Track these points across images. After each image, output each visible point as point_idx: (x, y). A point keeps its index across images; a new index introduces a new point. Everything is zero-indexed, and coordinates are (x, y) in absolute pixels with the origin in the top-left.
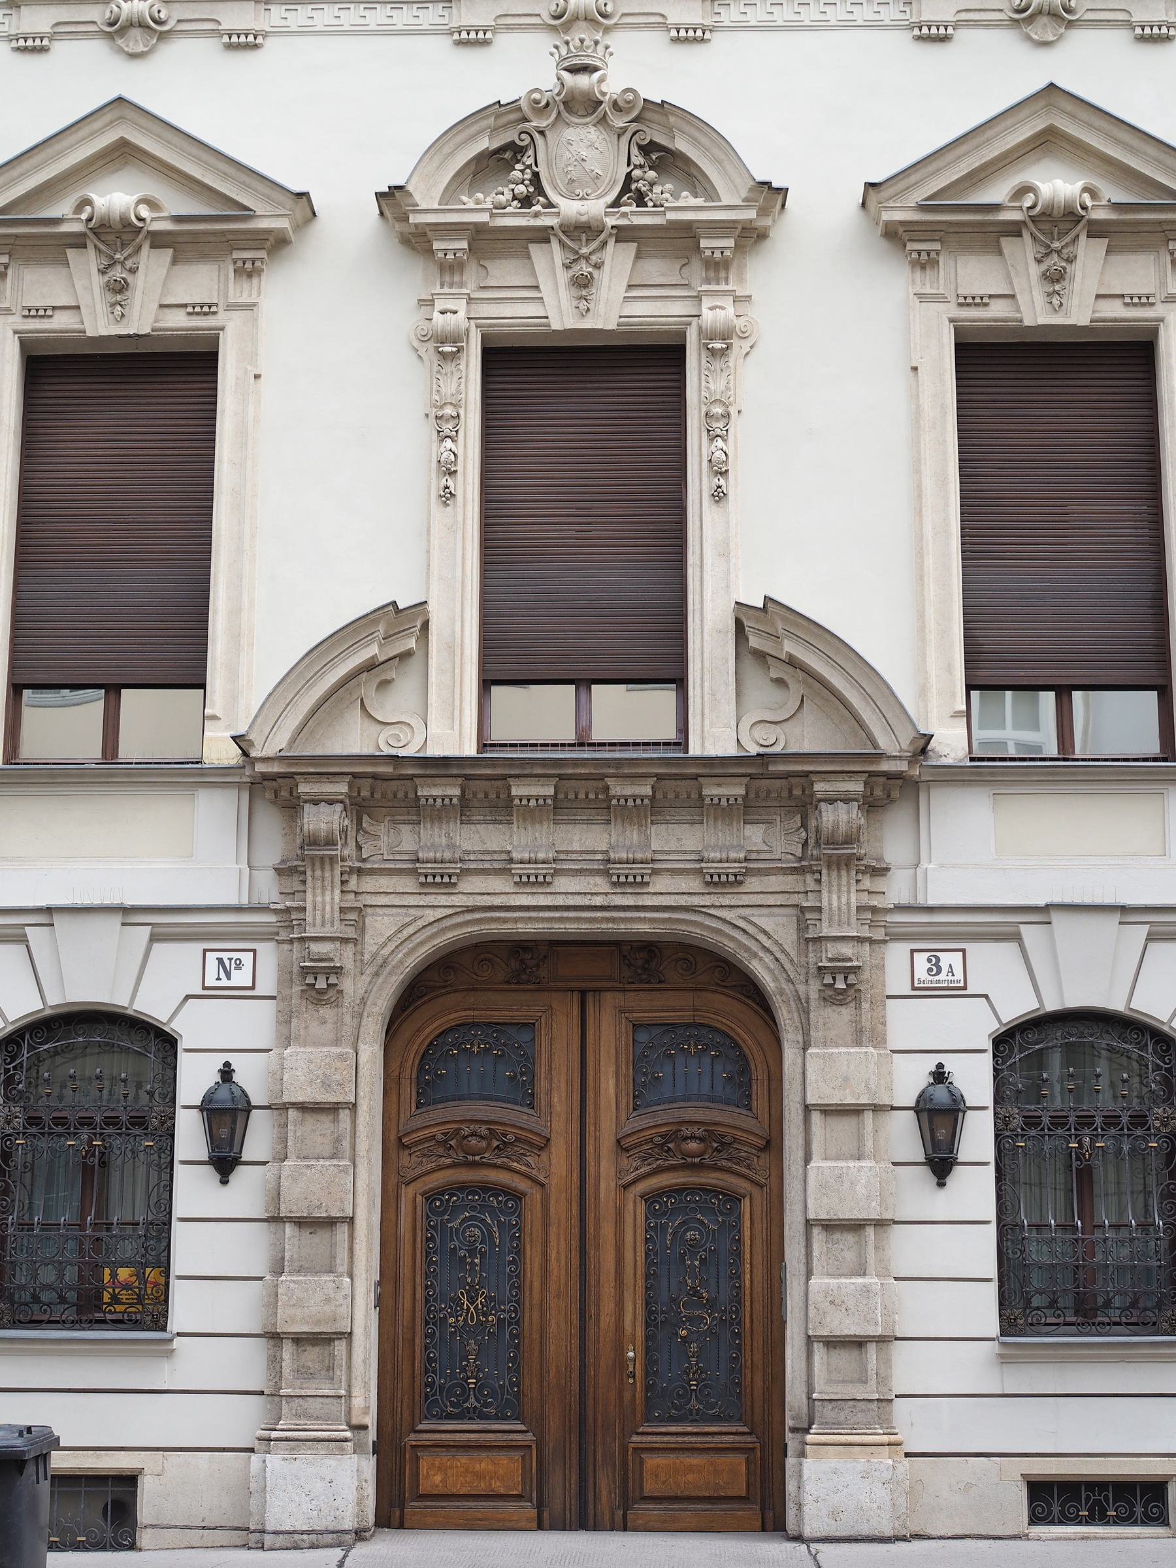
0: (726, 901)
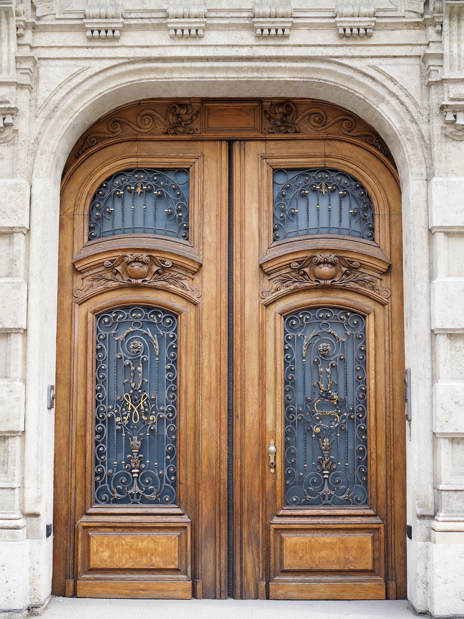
0: (357, 52)
